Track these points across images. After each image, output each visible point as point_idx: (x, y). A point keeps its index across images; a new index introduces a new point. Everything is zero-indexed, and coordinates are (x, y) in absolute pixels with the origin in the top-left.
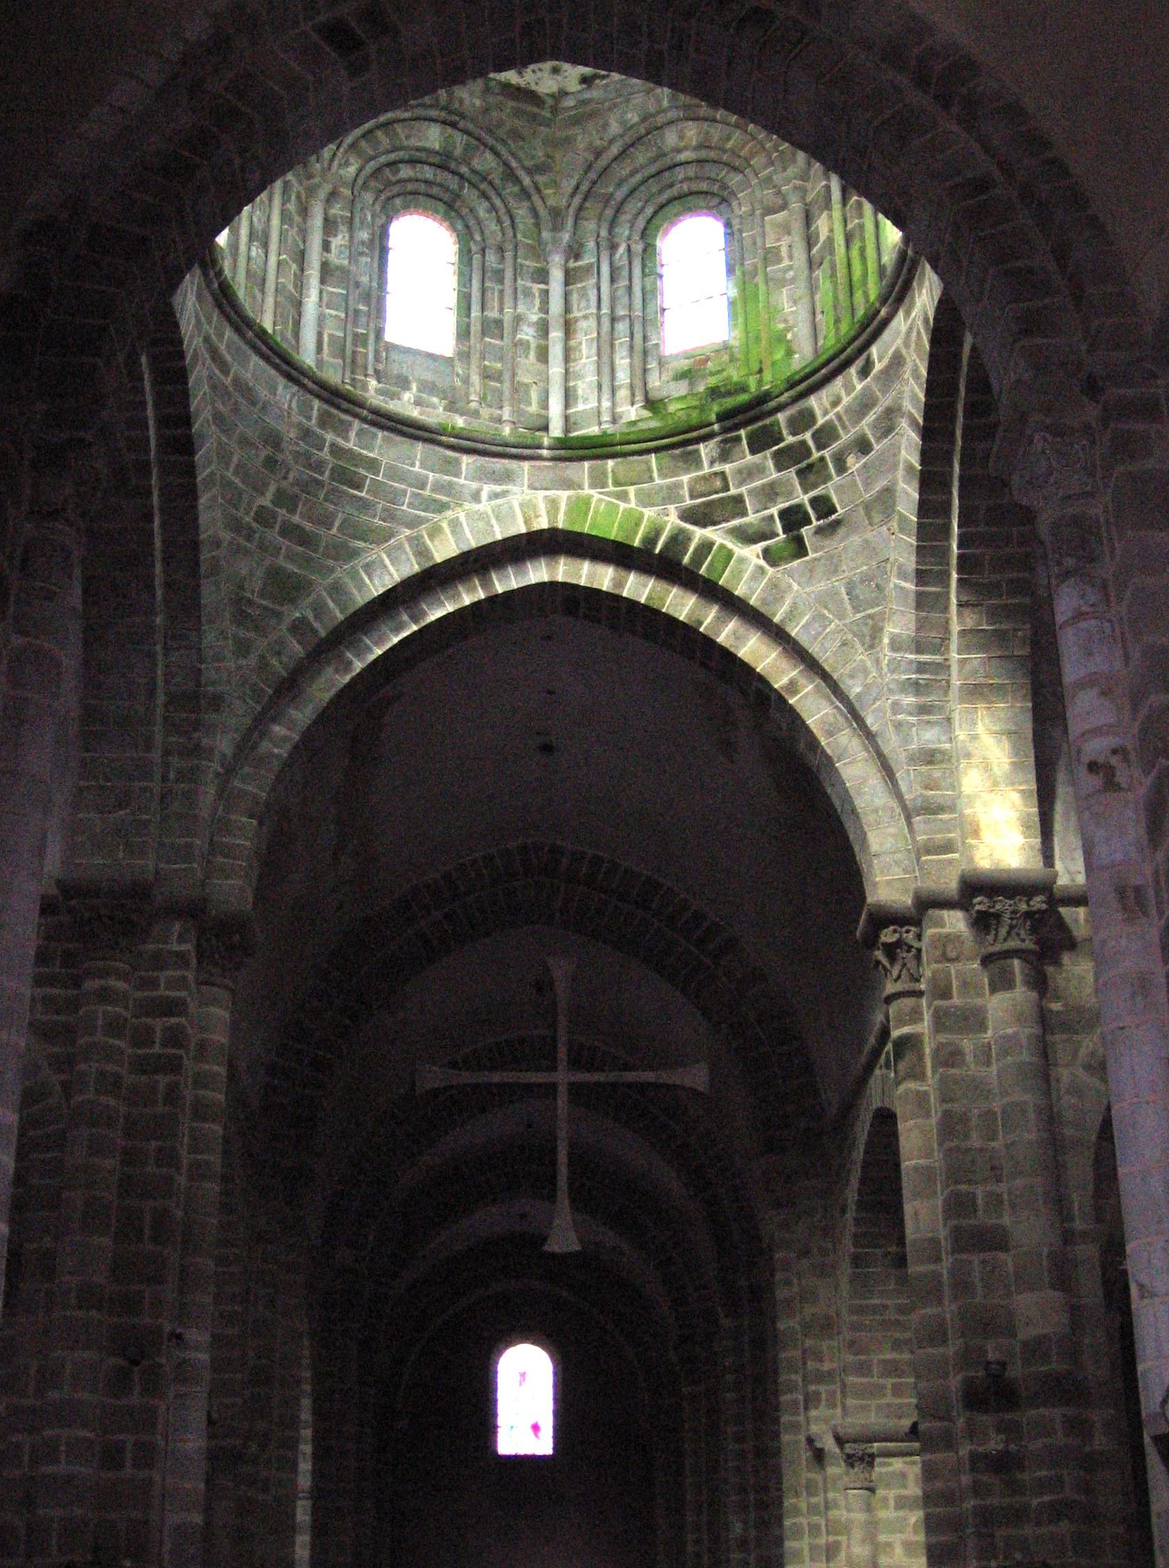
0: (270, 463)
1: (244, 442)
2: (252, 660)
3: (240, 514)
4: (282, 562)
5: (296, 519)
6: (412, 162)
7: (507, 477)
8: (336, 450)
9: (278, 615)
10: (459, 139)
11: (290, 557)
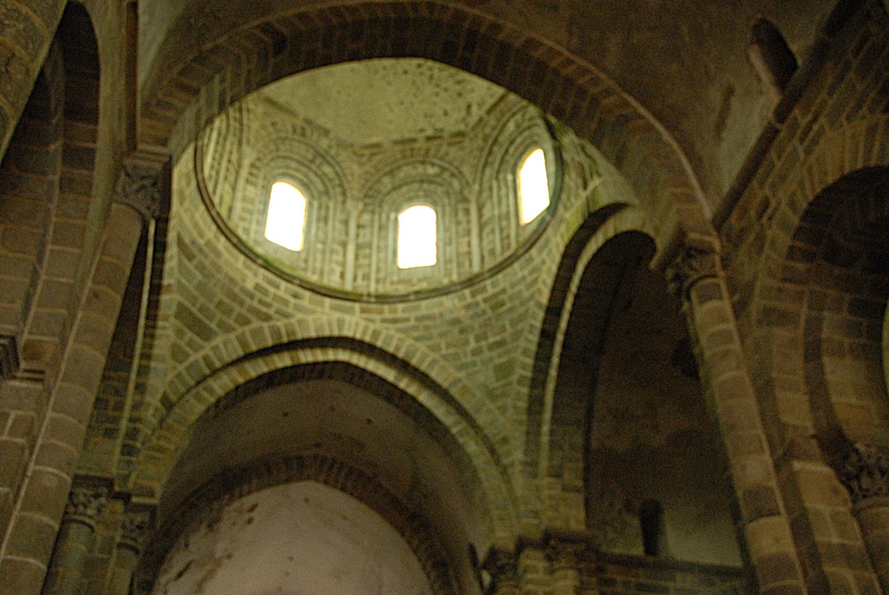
0: (462, 331)
1: (442, 335)
2: (511, 411)
3: (463, 360)
4: (497, 361)
5: (491, 340)
6: (512, 143)
7: (548, 241)
8: (485, 300)
9: (510, 384)
10: (518, 116)
11: (499, 357)
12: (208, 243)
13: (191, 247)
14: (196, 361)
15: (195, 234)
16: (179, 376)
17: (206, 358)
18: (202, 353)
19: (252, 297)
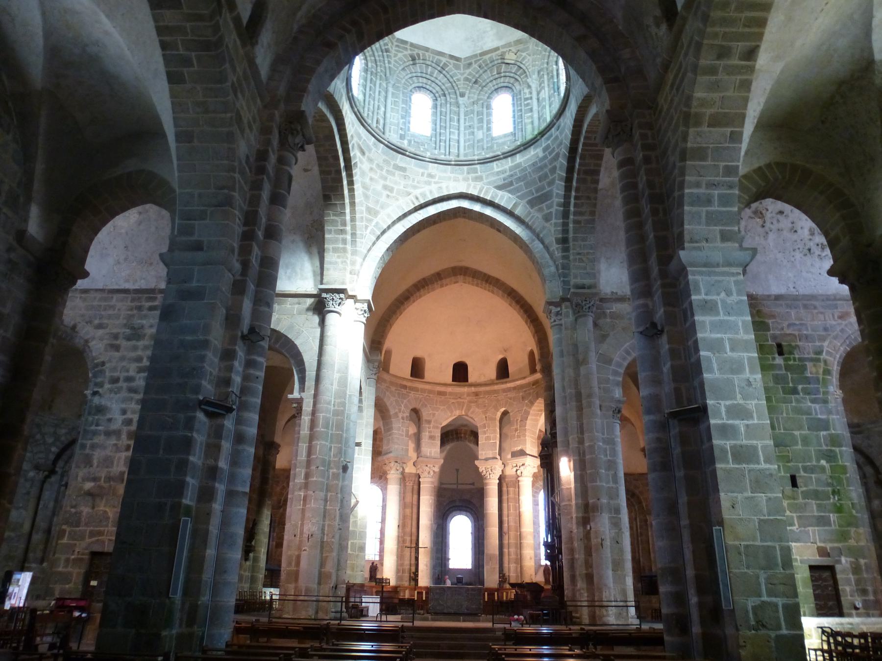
12: (511, 169)
13: (506, 182)
14: (556, 210)
15: (502, 176)
16: (555, 224)
17: (559, 205)
18: (555, 204)
19: (545, 157)
